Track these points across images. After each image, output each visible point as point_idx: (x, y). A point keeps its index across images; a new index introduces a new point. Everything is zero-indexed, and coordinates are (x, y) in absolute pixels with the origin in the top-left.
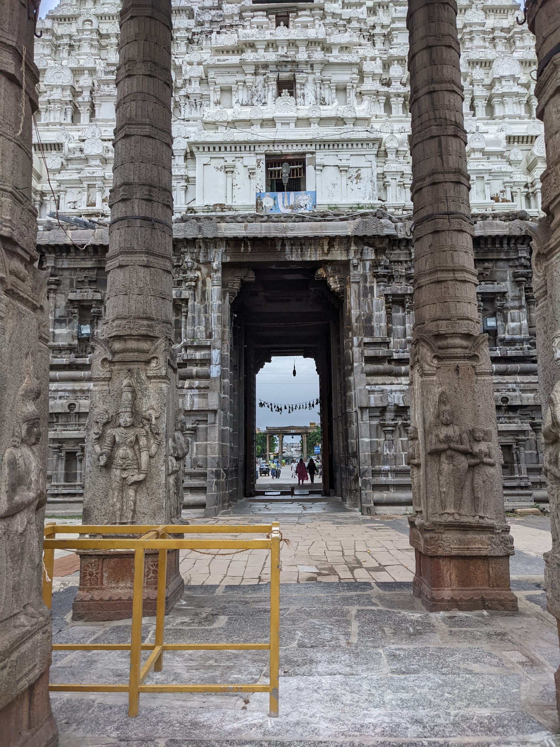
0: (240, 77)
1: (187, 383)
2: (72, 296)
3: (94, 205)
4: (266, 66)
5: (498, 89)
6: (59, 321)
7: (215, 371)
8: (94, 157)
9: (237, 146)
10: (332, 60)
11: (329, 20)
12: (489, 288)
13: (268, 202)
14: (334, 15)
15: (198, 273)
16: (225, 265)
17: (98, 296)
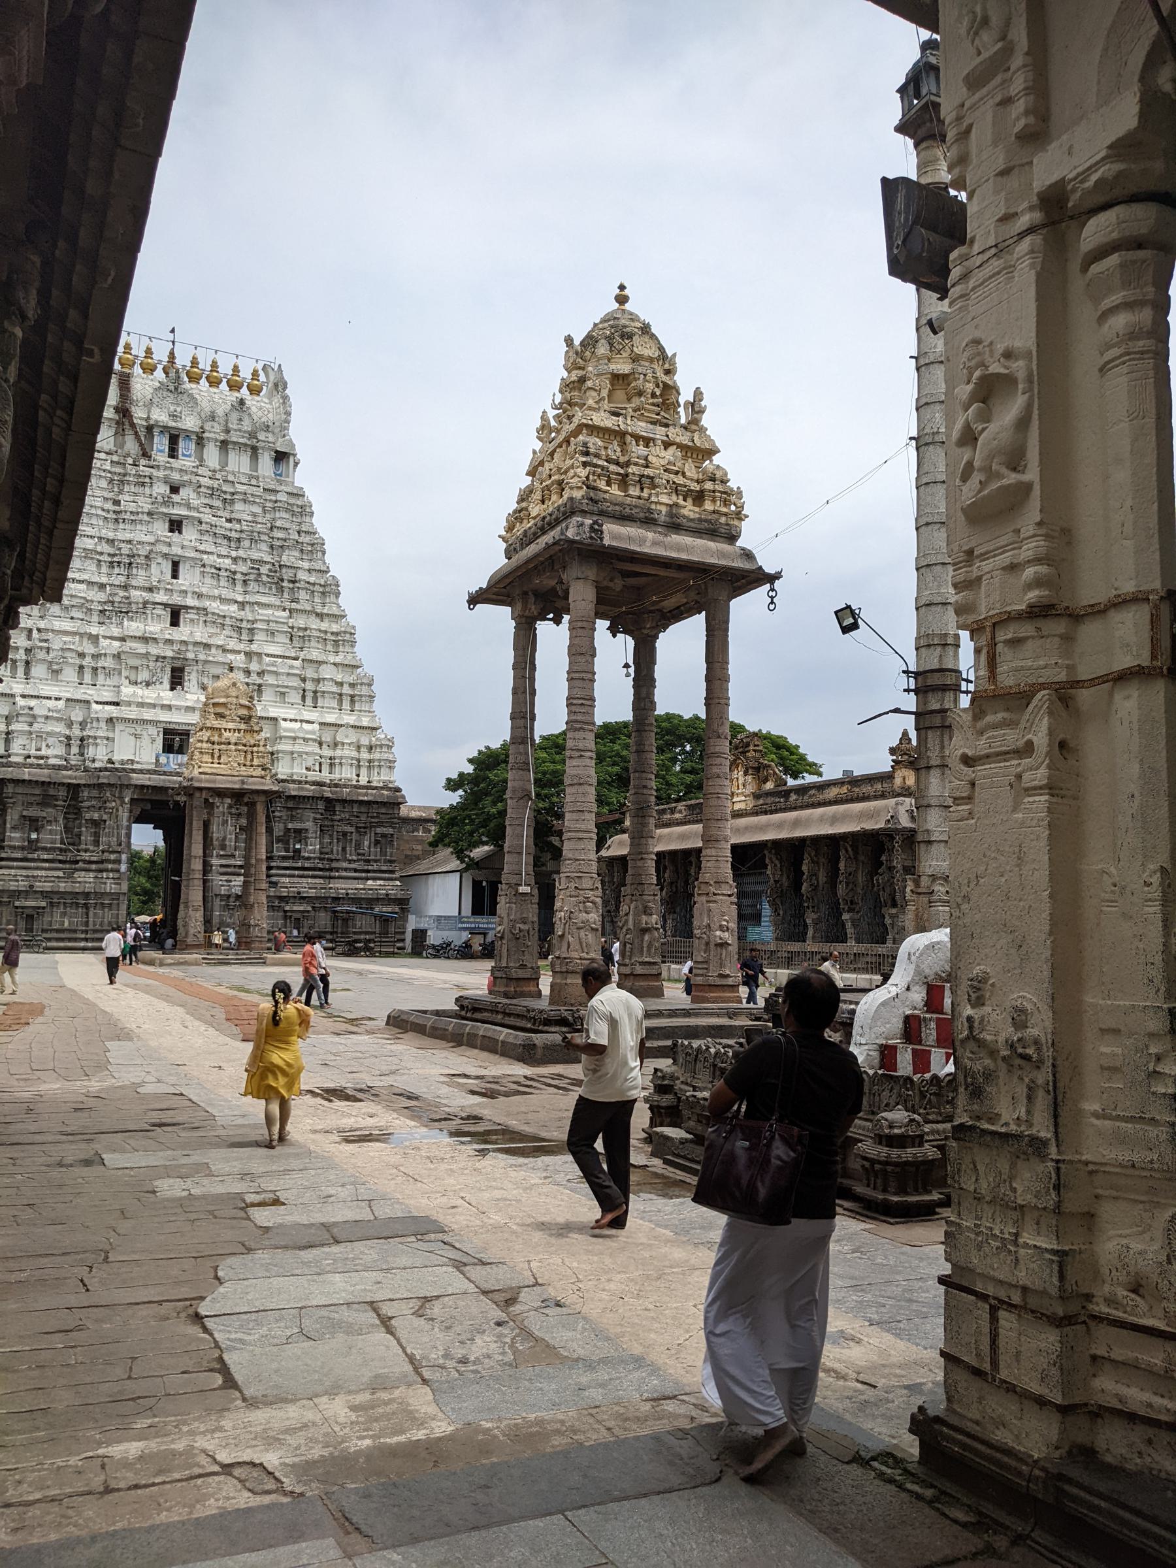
0: (144, 662)
1: (105, 875)
2: (25, 813)
3: (39, 750)
4: (164, 658)
5: (321, 687)
6: (14, 828)
7: (123, 868)
8: (41, 716)
9: (144, 722)
10: (211, 658)
11: (210, 618)
12: (298, 826)
13: (163, 760)
14: (213, 614)
15: (114, 804)
16: (132, 799)
17: (44, 814)
